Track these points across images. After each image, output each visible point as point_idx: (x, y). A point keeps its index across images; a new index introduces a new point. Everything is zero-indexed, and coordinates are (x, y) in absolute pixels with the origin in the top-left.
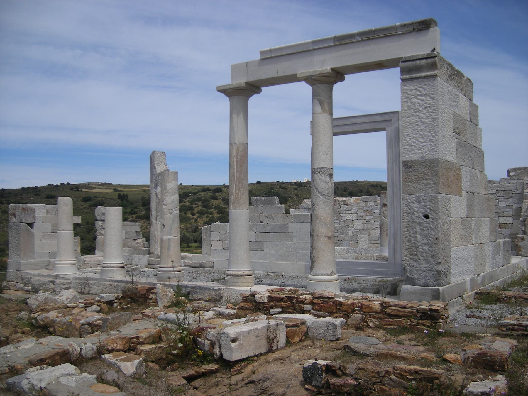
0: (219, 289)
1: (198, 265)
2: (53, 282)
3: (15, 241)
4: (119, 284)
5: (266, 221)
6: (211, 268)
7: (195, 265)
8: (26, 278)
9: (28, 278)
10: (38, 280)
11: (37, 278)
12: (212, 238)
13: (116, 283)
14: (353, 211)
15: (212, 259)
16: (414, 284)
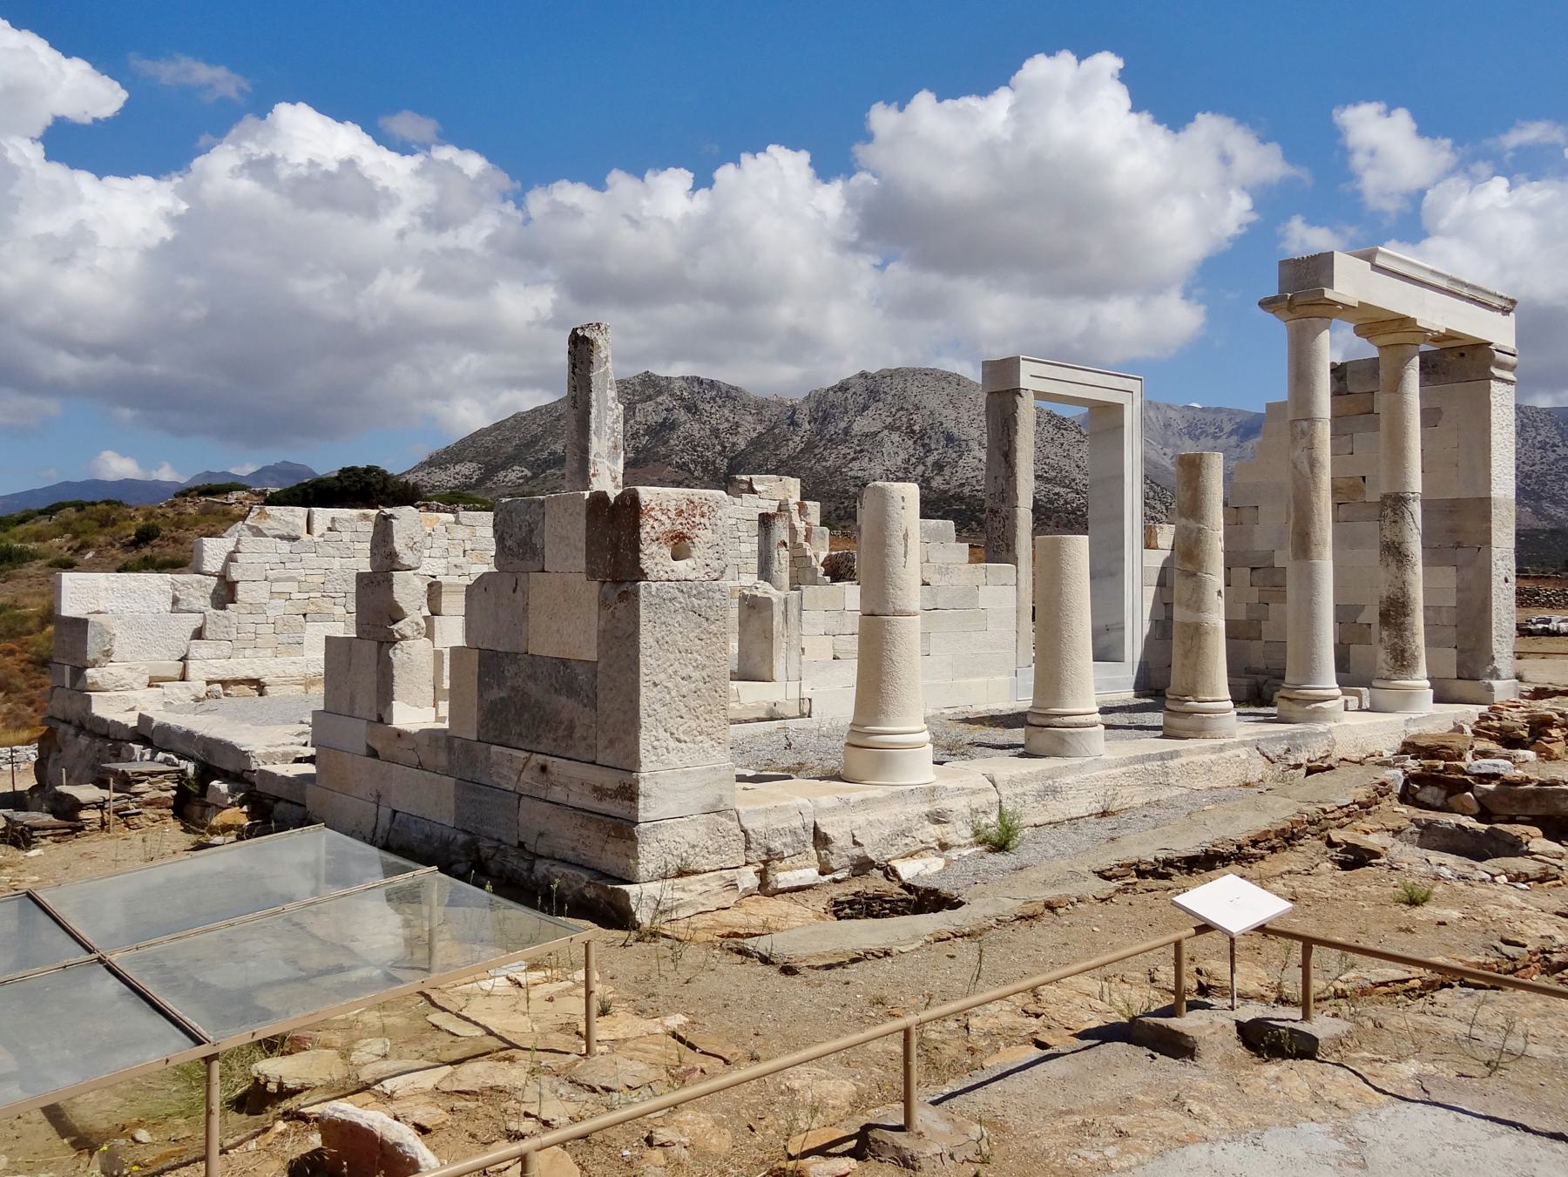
0: (1329, 731)
1: (762, 715)
2: (937, 818)
3: (689, 670)
4: (1148, 765)
5: (934, 579)
6: (802, 715)
7: (752, 716)
8: (780, 833)
9: (794, 832)
10: (870, 824)
11: (860, 818)
12: (806, 629)
13: (1139, 767)
14: (436, 552)
15: (807, 693)
16: (1498, 678)
